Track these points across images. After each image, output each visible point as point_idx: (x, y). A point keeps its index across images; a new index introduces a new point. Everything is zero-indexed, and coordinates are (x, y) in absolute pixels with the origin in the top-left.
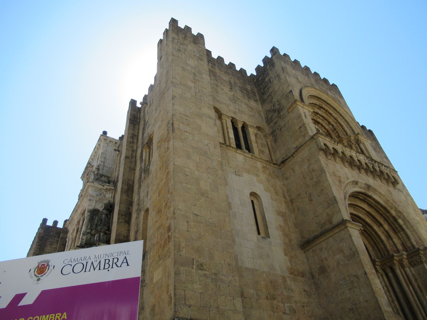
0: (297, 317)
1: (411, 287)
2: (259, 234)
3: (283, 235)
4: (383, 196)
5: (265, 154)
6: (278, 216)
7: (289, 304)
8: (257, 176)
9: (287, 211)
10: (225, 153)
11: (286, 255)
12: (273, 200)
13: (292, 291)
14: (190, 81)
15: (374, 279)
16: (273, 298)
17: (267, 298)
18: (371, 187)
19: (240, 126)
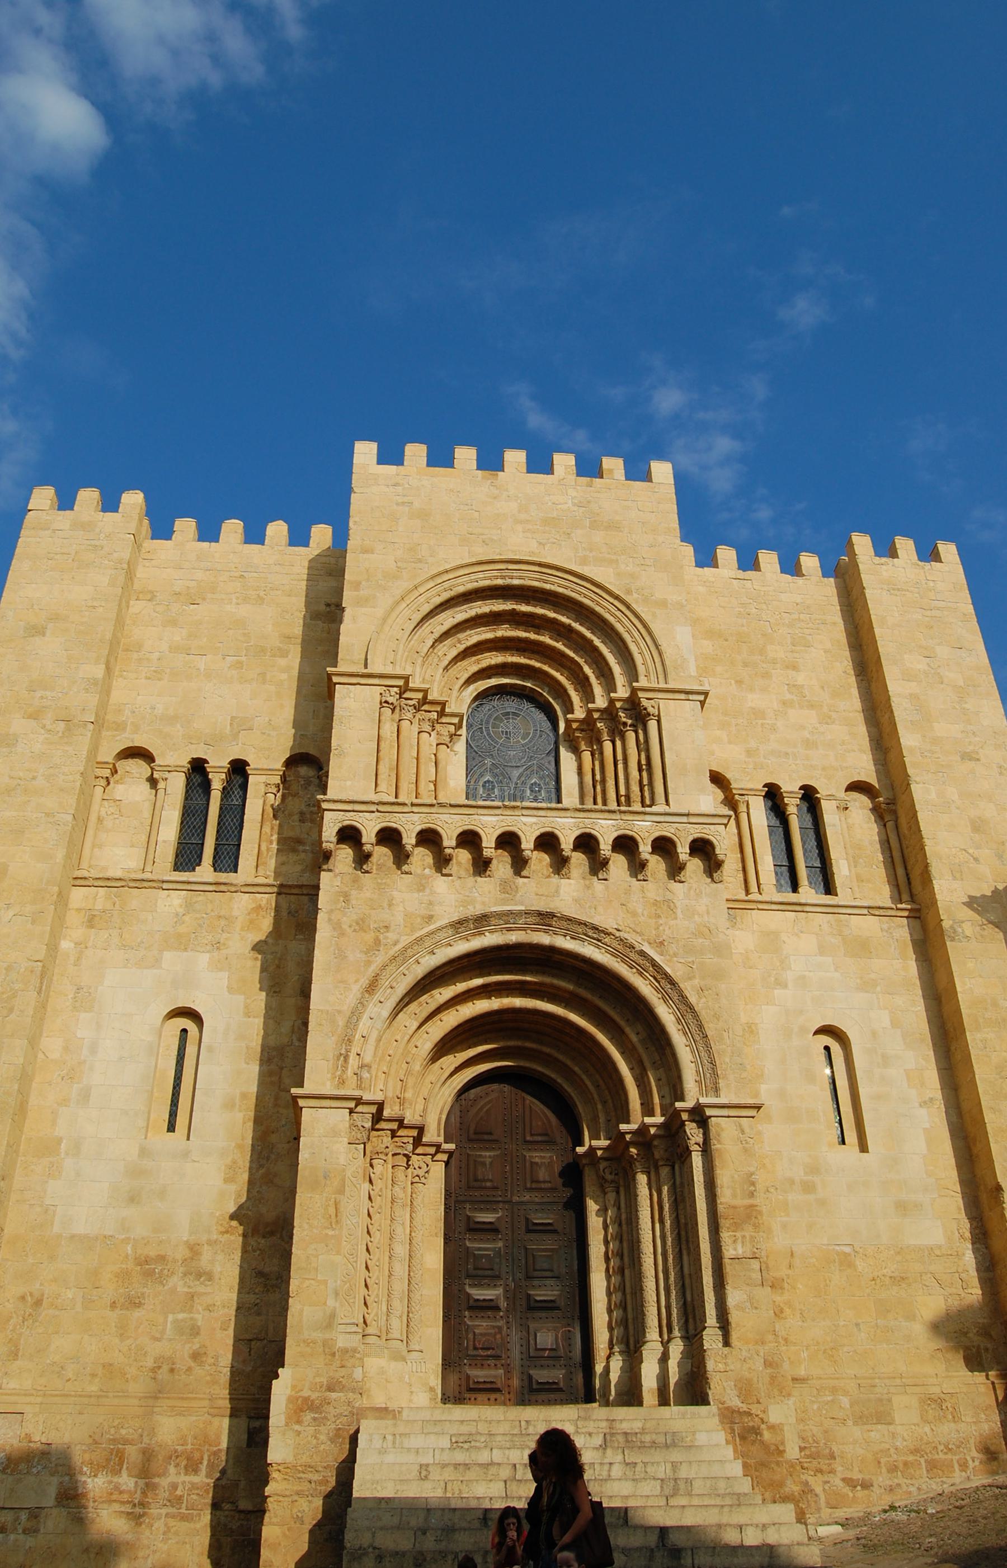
0: (198, 1346)
1: (657, 1226)
2: (171, 1128)
3: (244, 1123)
4: (609, 934)
5: (301, 848)
6: (248, 1064)
7: (181, 1316)
8: (217, 945)
9: (294, 1038)
10: (118, 903)
11: (227, 1180)
12: (249, 1017)
13: (210, 1276)
14: (24, 718)
15: (317, 1256)
16: (135, 1303)
17: (113, 1305)
18: (555, 916)
19: (217, 782)
